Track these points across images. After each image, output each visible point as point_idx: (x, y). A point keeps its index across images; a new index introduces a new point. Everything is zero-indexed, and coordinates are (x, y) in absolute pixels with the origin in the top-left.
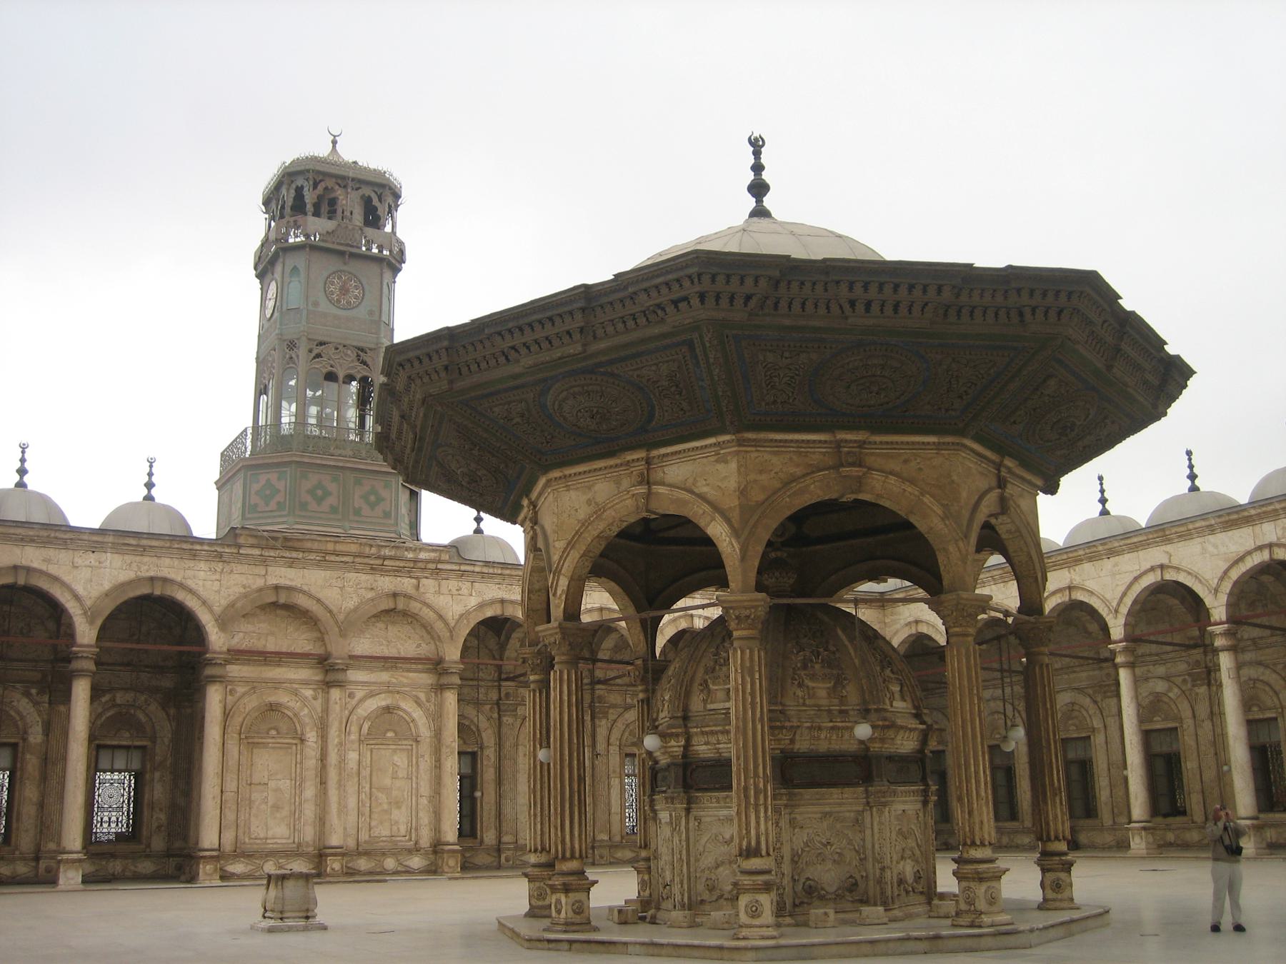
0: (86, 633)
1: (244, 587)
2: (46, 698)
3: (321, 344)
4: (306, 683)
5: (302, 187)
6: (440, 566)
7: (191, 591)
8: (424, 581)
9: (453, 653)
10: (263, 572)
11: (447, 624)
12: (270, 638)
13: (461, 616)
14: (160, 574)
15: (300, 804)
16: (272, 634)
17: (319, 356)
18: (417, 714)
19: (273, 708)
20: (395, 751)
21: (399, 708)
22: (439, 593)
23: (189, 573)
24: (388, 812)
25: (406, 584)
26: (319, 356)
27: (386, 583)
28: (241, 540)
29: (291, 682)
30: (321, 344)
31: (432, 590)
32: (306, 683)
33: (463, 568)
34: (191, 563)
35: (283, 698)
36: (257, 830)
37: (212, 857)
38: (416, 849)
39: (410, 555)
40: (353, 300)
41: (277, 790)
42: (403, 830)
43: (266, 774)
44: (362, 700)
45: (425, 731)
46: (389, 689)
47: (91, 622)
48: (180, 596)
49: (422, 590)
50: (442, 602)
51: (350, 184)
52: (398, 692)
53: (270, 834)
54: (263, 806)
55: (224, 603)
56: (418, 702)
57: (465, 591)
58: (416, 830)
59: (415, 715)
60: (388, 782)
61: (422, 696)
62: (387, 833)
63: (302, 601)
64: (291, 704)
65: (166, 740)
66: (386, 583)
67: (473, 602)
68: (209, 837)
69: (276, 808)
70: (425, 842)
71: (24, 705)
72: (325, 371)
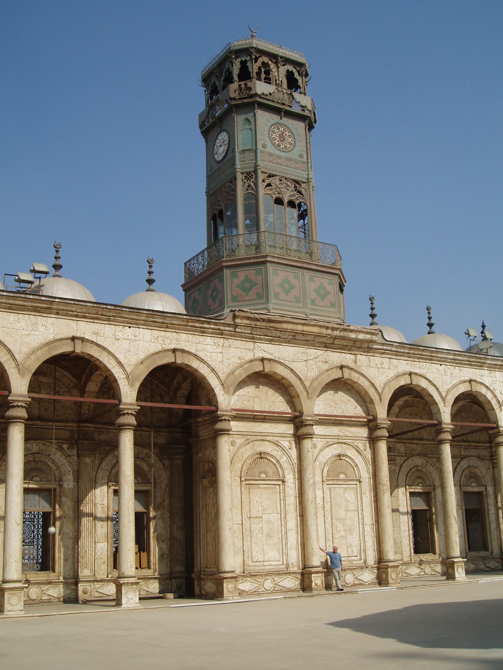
0: (128, 394)
1: (240, 359)
2: (75, 452)
3: (271, 176)
5: (246, 61)
7: (202, 361)
8: (359, 357)
10: (252, 347)
11: (376, 390)
12: (256, 400)
13: (385, 384)
14: (179, 347)
15: (286, 532)
16: (258, 397)
17: (269, 185)
18: (359, 460)
19: (261, 455)
20: (345, 489)
21: (346, 456)
22: (369, 366)
23: (200, 346)
24: (345, 537)
26: (269, 185)
27: (336, 357)
28: (238, 321)
29: (273, 435)
30: (271, 176)
31: (365, 364)
32: (283, 436)
34: (201, 339)
35: (267, 448)
36: (258, 556)
37: (232, 578)
38: (365, 567)
39: (353, 336)
40: (288, 146)
41: (269, 522)
43: (260, 509)
44: (322, 450)
45: (365, 474)
46: (340, 441)
47: (131, 385)
48: (195, 364)
49: (358, 363)
50: (371, 373)
51: (280, 60)
52: (345, 443)
53: (266, 557)
54: (260, 535)
55: (227, 371)
57: (386, 365)
58: (365, 551)
60: (342, 513)
63: (281, 371)
64: (274, 453)
65: (163, 486)
67: (392, 373)
68: (230, 561)
69: (269, 536)
71: (58, 457)
72: (274, 196)
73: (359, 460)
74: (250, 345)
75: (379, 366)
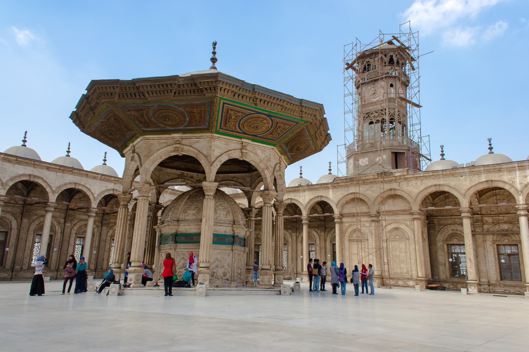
4: (367, 222)
6: (405, 177)
9: (416, 208)
18: (407, 229)
20: (400, 243)
22: (408, 186)
25: (394, 185)
27: (387, 186)
28: (338, 182)
33: (415, 176)
42: (405, 271)
46: (395, 222)
49: (401, 186)
56: (407, 225)
59: (406, 230)
60: (398, 254)
61: (408, 223)
62: (399, 272)
66: (387, 186)
67: (423, 187)
70: (415, 277)
72: (369, 122)
73: (407, 229)
74: (347, 189)
75: (414, 185)
